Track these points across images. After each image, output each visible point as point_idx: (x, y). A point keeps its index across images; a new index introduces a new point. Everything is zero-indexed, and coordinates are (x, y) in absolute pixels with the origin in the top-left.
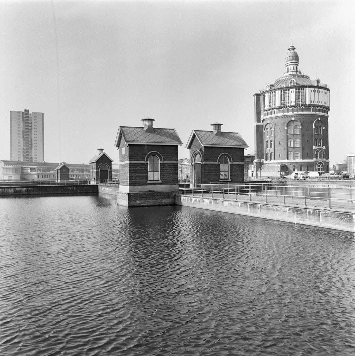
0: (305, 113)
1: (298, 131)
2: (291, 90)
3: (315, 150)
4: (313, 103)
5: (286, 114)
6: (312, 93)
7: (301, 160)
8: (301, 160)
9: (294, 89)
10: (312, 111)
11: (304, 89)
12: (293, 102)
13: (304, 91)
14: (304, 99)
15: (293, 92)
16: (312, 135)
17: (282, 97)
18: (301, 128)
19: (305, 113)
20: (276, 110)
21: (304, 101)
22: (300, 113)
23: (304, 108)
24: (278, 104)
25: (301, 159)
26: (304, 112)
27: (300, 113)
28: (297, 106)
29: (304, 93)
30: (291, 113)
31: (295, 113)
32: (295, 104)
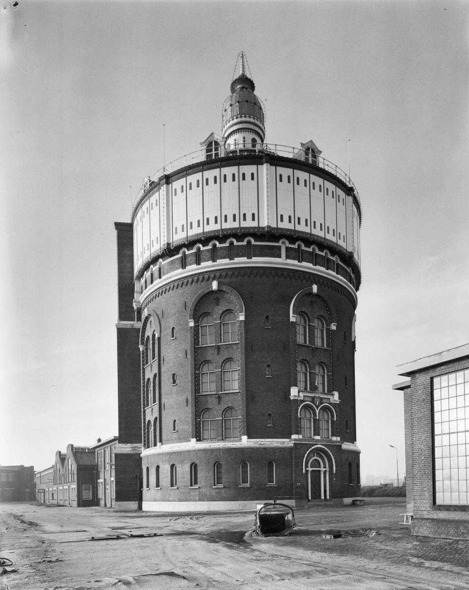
0: (259, 261)
1: (234, 335)
3: (297, 402)
4: (285, 225)
6: (284, 186)
7: (245, 442)
8: (245, 442)
10: (287, 257)
16: (285, 348)
18: (242, 318)
19: (259, 261)
22: (241, 261)
25: (245, 438)
26: (254, 259)
27: (241, 261)
31: (224, 263)
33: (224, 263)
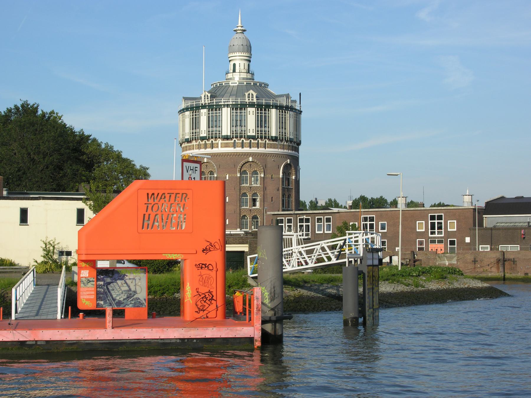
2: (249, 109)
5: (239, 150)
9: (254, 109)
11: (268, 111)
12: (251, 131)
13: (269, 114)
14: (268, 127)
15: (251, 113)
17: (233, 120)
20: (220, 141)
21: (269, 132)
22: (261, 150)
23: (267, 141)
24: (226, 131)
27: (261, 150)
28: (258, 138)
29: (269, 116)
30: (246, 150)
31: (254, 150)
32: (254, 134)
33: (254, 150)
